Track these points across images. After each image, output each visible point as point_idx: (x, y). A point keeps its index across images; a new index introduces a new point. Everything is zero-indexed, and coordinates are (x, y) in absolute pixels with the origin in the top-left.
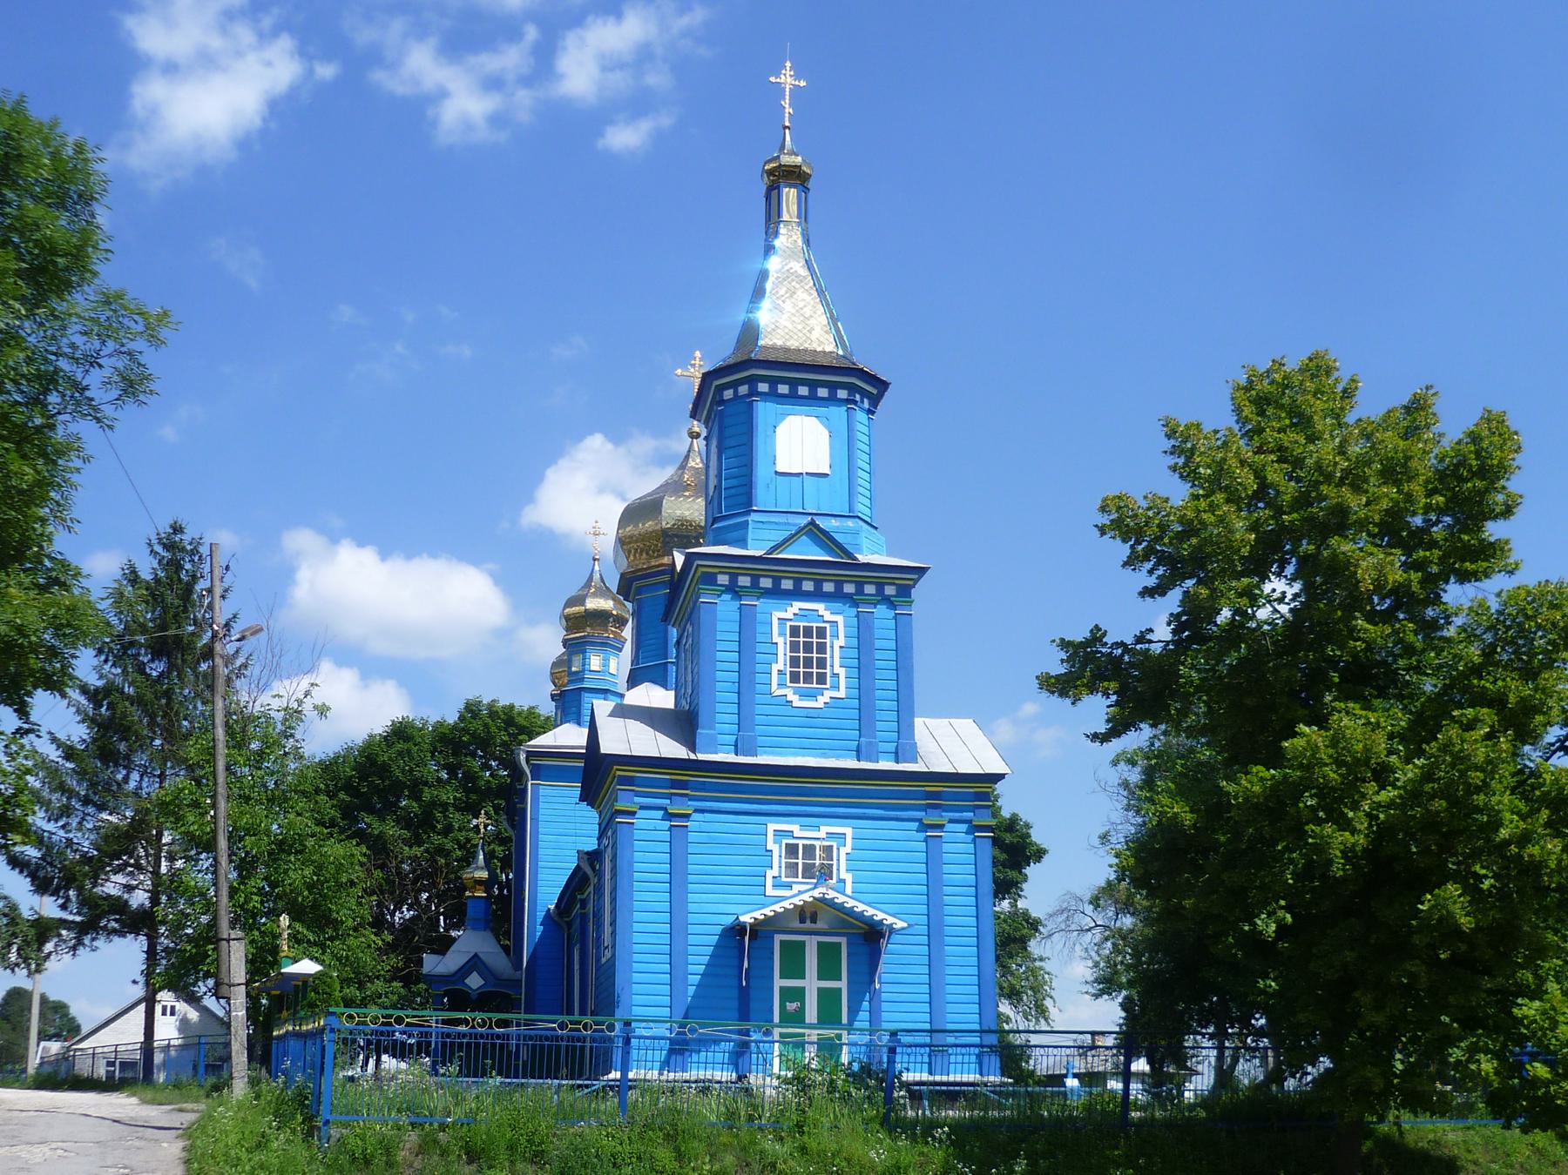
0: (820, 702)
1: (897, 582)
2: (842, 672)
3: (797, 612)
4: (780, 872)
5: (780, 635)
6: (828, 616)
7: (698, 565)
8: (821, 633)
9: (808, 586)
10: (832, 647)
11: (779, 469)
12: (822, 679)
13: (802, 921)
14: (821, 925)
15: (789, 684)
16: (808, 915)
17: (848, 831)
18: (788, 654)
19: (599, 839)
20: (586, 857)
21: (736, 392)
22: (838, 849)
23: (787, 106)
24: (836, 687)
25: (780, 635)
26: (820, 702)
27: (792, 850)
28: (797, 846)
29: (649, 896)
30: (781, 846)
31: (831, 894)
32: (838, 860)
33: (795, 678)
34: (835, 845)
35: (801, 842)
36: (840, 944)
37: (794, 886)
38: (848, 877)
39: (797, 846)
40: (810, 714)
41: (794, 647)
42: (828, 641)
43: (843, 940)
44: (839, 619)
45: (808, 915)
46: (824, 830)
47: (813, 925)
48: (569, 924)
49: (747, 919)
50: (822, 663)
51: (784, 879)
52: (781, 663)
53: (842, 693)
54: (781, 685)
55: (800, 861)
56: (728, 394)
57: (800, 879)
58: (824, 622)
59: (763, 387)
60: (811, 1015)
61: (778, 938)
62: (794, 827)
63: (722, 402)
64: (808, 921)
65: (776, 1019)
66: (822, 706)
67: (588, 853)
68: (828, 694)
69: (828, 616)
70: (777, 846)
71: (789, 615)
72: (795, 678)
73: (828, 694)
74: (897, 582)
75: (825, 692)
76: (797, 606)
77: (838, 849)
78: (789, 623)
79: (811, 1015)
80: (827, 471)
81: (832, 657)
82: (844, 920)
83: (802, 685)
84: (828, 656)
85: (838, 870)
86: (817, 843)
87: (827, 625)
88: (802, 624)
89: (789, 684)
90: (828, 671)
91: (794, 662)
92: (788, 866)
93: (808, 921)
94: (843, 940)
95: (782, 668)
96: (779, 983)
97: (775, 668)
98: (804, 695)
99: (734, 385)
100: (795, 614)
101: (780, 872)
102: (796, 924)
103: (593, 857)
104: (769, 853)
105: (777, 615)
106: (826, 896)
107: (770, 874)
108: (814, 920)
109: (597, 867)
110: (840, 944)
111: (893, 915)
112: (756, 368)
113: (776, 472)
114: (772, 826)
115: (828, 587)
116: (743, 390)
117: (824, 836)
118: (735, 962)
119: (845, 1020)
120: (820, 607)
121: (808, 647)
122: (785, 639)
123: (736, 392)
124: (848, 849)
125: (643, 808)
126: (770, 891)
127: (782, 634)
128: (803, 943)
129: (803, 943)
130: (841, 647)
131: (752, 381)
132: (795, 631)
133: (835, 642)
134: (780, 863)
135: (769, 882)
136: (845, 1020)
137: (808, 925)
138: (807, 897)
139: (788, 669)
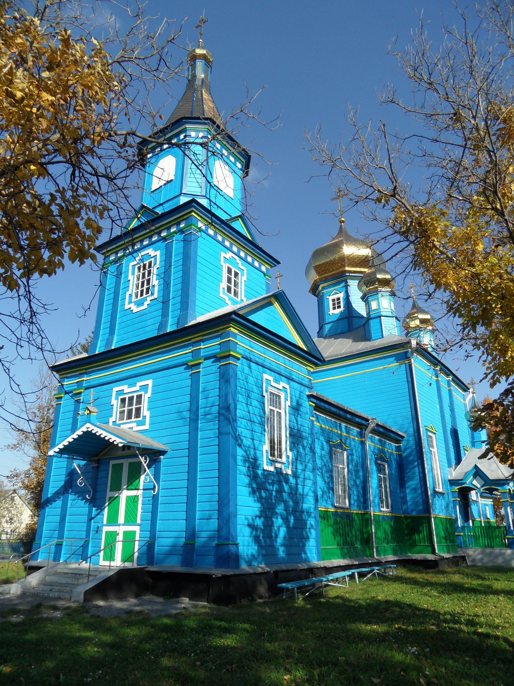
1: (185, 217)
17: (150, 382)
24: (152, 294)
44: (158, 253)
46: (139, 384)
54: (130, 302)
60: (121, 519)
62: (125, 388)
79: (121, 519)
119: (139, 521)
124: (149, 394)
136: (139, 521)
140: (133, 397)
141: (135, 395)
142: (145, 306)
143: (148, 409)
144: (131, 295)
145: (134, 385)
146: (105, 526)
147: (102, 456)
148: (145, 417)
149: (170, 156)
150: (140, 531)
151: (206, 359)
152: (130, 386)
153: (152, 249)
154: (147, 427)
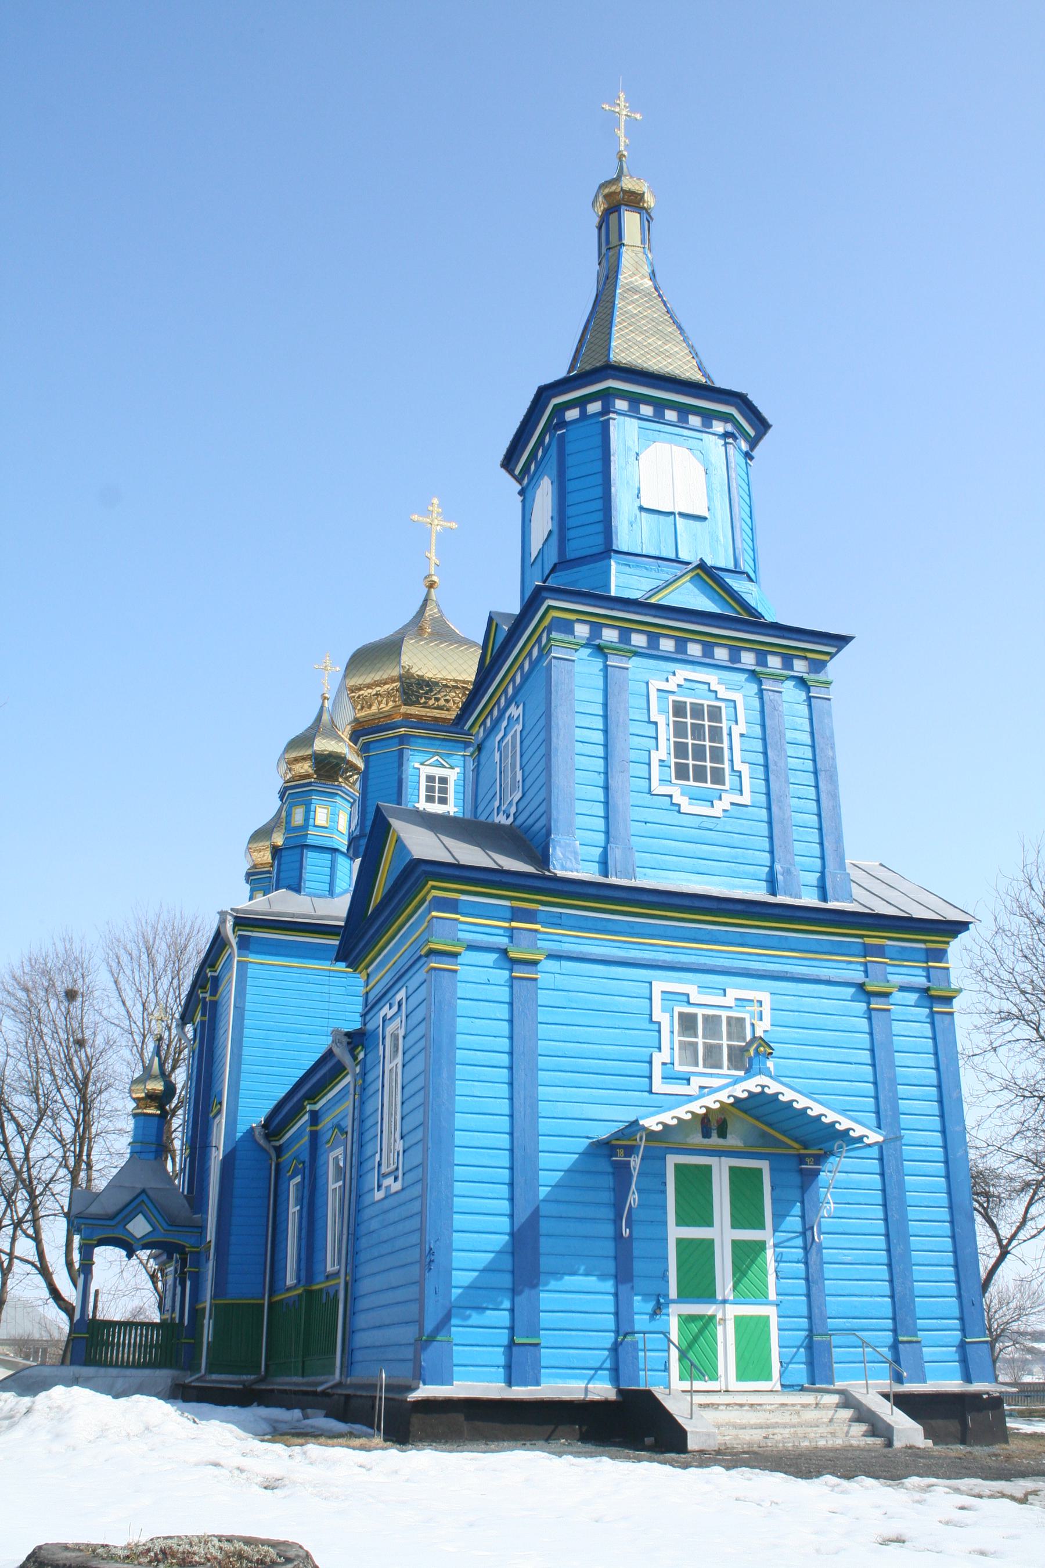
1: (809, 655)
2: (745, 769)
3: (682, 682)
4: (672, 1056)
5: (660, 711)
7: (550, 607)
8: (715, 714)
10: (730, 734)
11: (645, 506)
12: (718, 777)
13: (706, 1134)
14: (733, 1141)
15: (674, 781)
16: (714, 1124)
18: (672, 739)
19: (364, 1015)
20: (345, 1040)
21: (583, 412)
22: (753, 1025)
23: (623, 139)
25: (660, 711)
26: (717, 811)
27: (688, 1023)
28: (694, 1016)
29: (478, 1089)
31: (773, 1088)
33: (682, 772)
35: (700, 1012)
36: (760, 1171)
37: (693, 1079)
39: (694, 1016)
40: (705, 825)
41: (679, 730)
43: (764, 1165)
44: (737, 696)
45: (714, 1124)
46: (733, 994)
48: (279, 1151)
49: (652, 1123)
50: (717, 755)
51: (678, 1067)
52: (664, 751)
53: (746, 799)
55: (700, 1041)
56: (572, 414)
57: (700, 1069)
58: (717, 698)
59: (621, 405)
62: (692, 990)
63: (563, 424)
64: (714, 1134)
65: (673, 1294)
66: (720, 814)
67: (348, 1034)
68: (728, 798)
70: (668, 1015)
71: (671, 686)
72: (682, 772)
74: (809, 655)
76: (684, 673)
78: (671, 698)
81: (731, 749)
82: (764, 1135)
83: (691, 783)
84: (725, 745)
86: (724, 1014)
87: (722, 705)
88: (689, 700)
89: (674, 781)
91: (680, 750)
92: (683, 1045)
93: (714, 1134)
95: (664, 757)
96: (675, 1232)
99: (582, 403)
100: (679, 686)
101: (672, 1056)
102: (697, 1139)
103: (357, 1040)
104: (655, 1027)
106: (766, 1090)
107: (658, 1059)
108: (722, 1134)
109: (361, 1056)
112: (615, 378)
113: (642, 509)
114: (662, 984)
116: (594, 407)
117: (732, 1003)
118: (607, 1197)
119: (772, 1296)
120: (711, 677)
121: (697, 731)
123: (583, 412)
125: (471, 947)
126: (658, 1086)
128: (708, 1169)
129: (708, 1169)
130: (742, 735)
131: (607, 397)
132: (679, 709)
133: (734, 727)
134: (672, 1042)
135: (657, 1072)
136: (772, 1296)
137: (715, 1141)
138: (724, 1097)
139: (673, 760)
142: (717, 811)
146: (674, 1302)
150: (779, 1317)
151: (903, 989)
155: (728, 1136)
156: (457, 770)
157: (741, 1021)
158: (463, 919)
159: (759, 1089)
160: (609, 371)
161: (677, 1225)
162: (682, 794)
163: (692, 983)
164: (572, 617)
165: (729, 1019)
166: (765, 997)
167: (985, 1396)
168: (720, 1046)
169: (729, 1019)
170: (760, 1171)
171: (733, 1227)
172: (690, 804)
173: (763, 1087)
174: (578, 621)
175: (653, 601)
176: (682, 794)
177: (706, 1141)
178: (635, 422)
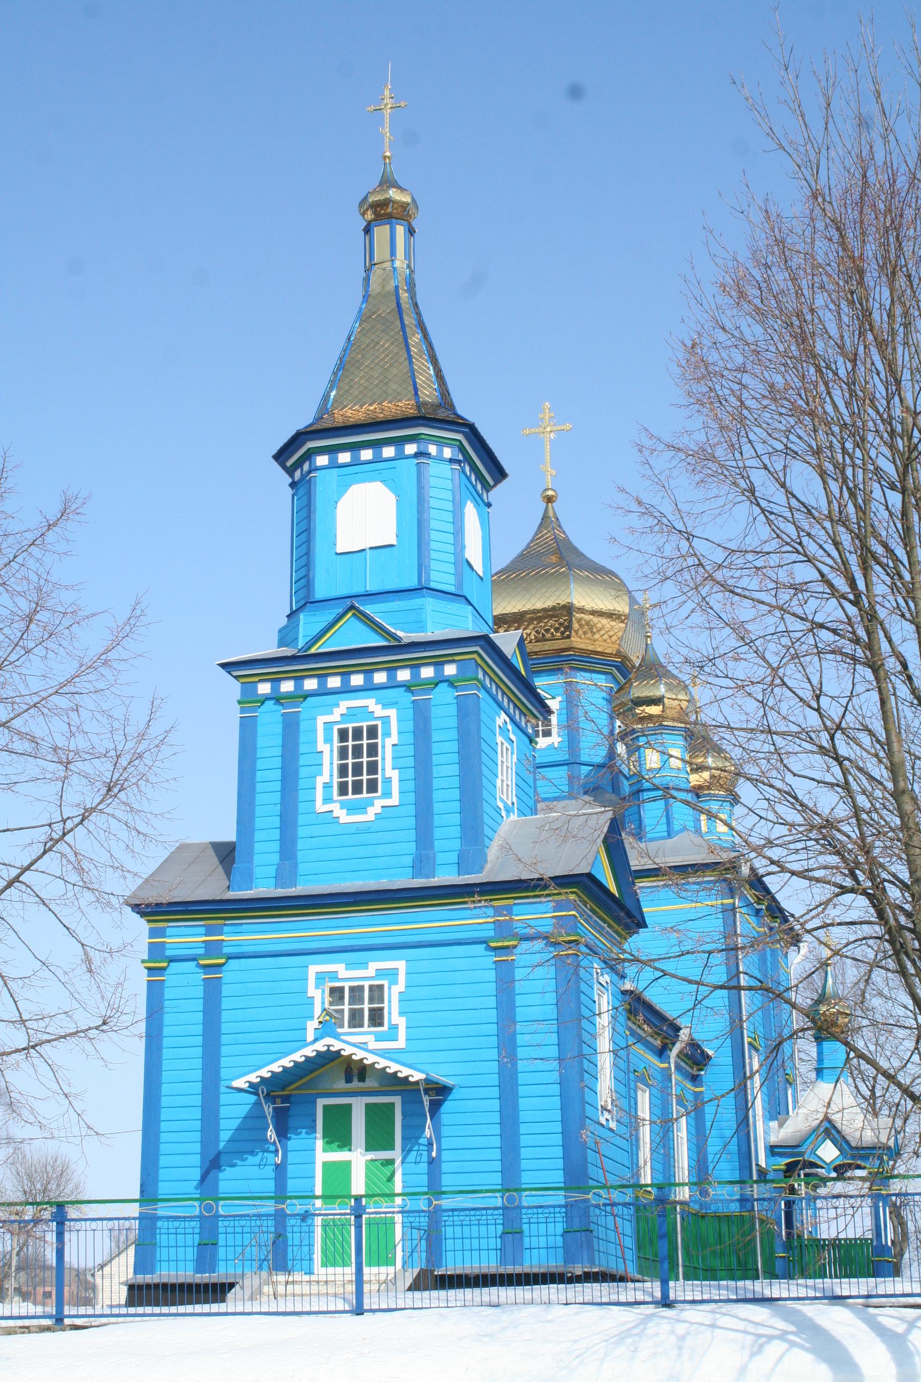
0: (370, 815)
1: (457, 658)
6: (379, 711)
8: (373, 732)
9: (357, 680)
10: (383, 747)
11: (338, 551)
12: (373, 786)
13: (349, 1080)
16: (355, 1072)
17: (401, 965)
22: (390, 988)
24: (387, 794)
26: (370, 815)
28: (342, 989)
30: (323, 991)
32: (390, 1001)
34: (385, 983)
35: (347, 985)
38: (401, 1022)
39: (342, 989)
42: (379, 741)
43: (397, 1100)
44: (392, 713)
45: (355, 1072)
46: (373, 967)
47: (361, 1084)
50: (373, 768)
53: (395, 800)
54: (328, 800)
55: (346, 1007)
59: (322, 460)
61: (321, 1103)
62: (340, 969)
64: (355, 1079)
68: (379, 804)
69: (379, 711)
71: (336, 717)
73: (379, 804)
75: (376, 802)
76: (345, 704)
77: (390, 988)
80: (395, 543)
81: (383, 759)
85: (390, 1013)
86: (366, 984)
90: (379, 776)
93: (355, 1079)
94: (397, 1100)
95: (328, 781)
97: (320, 781)
98: (352, 809)
102: (341, 1085)
105: (321, 720)
106: (332, 1049)
108: (362, 1079)
110: (393, 1104)
111: (409, 1066)
112: (311, 440)
113: (337, 554)
115: (380, 678)
120: (370, 702)
122: (332, 747)
124: (401, 986)
127: (328, 740)
128: (349, 1106)
129: (349, 1106)
130: (393, 745)
137: (356, 1084)
140: (361, 988)
141: (366, 984)
143: (401, 1013)
144: (327, 786)
145: (364, 965)
147: (294, 1089)
148: (395, 1027)
149: (379, 483)
152: (350, 966)
153: (374, 701)
154: (401, 1043)
155: (367, 1080)
156: (559, 699)
157: (381, 987)
158: (168, 941)
159: (325, 1048)
160: (303, 437)
161: (324, 1151)
162: (341, 808)
163: (340, 962)
164: (256, 679)
165: (371, 987)
166: (401, 965)
167: (569, 1275)
168: (362, 1010)
169: (371, 987)
170: (393, 1105)
171: (394, 1149)
172: (347, 815)
173: (329, 1046)
174: (260, 681)
175: (313, 650)
176: (341, 808)
177: (349, 1085)
178: (335, 471)
